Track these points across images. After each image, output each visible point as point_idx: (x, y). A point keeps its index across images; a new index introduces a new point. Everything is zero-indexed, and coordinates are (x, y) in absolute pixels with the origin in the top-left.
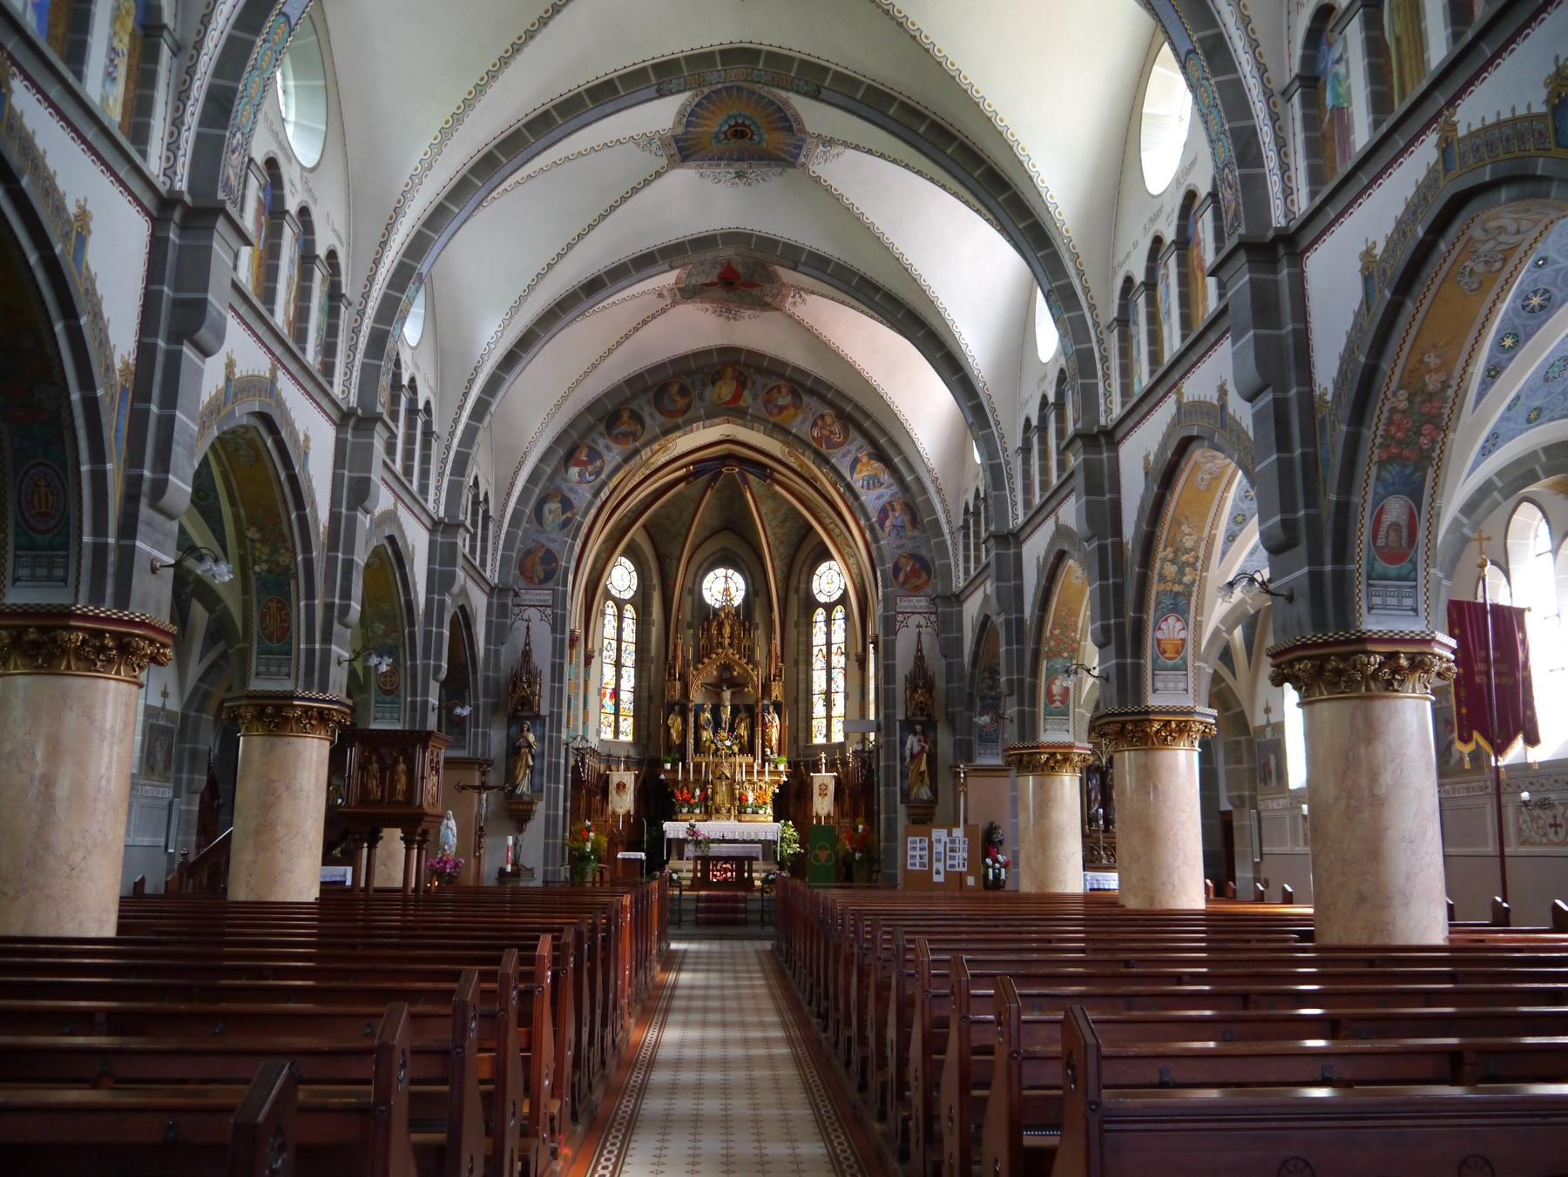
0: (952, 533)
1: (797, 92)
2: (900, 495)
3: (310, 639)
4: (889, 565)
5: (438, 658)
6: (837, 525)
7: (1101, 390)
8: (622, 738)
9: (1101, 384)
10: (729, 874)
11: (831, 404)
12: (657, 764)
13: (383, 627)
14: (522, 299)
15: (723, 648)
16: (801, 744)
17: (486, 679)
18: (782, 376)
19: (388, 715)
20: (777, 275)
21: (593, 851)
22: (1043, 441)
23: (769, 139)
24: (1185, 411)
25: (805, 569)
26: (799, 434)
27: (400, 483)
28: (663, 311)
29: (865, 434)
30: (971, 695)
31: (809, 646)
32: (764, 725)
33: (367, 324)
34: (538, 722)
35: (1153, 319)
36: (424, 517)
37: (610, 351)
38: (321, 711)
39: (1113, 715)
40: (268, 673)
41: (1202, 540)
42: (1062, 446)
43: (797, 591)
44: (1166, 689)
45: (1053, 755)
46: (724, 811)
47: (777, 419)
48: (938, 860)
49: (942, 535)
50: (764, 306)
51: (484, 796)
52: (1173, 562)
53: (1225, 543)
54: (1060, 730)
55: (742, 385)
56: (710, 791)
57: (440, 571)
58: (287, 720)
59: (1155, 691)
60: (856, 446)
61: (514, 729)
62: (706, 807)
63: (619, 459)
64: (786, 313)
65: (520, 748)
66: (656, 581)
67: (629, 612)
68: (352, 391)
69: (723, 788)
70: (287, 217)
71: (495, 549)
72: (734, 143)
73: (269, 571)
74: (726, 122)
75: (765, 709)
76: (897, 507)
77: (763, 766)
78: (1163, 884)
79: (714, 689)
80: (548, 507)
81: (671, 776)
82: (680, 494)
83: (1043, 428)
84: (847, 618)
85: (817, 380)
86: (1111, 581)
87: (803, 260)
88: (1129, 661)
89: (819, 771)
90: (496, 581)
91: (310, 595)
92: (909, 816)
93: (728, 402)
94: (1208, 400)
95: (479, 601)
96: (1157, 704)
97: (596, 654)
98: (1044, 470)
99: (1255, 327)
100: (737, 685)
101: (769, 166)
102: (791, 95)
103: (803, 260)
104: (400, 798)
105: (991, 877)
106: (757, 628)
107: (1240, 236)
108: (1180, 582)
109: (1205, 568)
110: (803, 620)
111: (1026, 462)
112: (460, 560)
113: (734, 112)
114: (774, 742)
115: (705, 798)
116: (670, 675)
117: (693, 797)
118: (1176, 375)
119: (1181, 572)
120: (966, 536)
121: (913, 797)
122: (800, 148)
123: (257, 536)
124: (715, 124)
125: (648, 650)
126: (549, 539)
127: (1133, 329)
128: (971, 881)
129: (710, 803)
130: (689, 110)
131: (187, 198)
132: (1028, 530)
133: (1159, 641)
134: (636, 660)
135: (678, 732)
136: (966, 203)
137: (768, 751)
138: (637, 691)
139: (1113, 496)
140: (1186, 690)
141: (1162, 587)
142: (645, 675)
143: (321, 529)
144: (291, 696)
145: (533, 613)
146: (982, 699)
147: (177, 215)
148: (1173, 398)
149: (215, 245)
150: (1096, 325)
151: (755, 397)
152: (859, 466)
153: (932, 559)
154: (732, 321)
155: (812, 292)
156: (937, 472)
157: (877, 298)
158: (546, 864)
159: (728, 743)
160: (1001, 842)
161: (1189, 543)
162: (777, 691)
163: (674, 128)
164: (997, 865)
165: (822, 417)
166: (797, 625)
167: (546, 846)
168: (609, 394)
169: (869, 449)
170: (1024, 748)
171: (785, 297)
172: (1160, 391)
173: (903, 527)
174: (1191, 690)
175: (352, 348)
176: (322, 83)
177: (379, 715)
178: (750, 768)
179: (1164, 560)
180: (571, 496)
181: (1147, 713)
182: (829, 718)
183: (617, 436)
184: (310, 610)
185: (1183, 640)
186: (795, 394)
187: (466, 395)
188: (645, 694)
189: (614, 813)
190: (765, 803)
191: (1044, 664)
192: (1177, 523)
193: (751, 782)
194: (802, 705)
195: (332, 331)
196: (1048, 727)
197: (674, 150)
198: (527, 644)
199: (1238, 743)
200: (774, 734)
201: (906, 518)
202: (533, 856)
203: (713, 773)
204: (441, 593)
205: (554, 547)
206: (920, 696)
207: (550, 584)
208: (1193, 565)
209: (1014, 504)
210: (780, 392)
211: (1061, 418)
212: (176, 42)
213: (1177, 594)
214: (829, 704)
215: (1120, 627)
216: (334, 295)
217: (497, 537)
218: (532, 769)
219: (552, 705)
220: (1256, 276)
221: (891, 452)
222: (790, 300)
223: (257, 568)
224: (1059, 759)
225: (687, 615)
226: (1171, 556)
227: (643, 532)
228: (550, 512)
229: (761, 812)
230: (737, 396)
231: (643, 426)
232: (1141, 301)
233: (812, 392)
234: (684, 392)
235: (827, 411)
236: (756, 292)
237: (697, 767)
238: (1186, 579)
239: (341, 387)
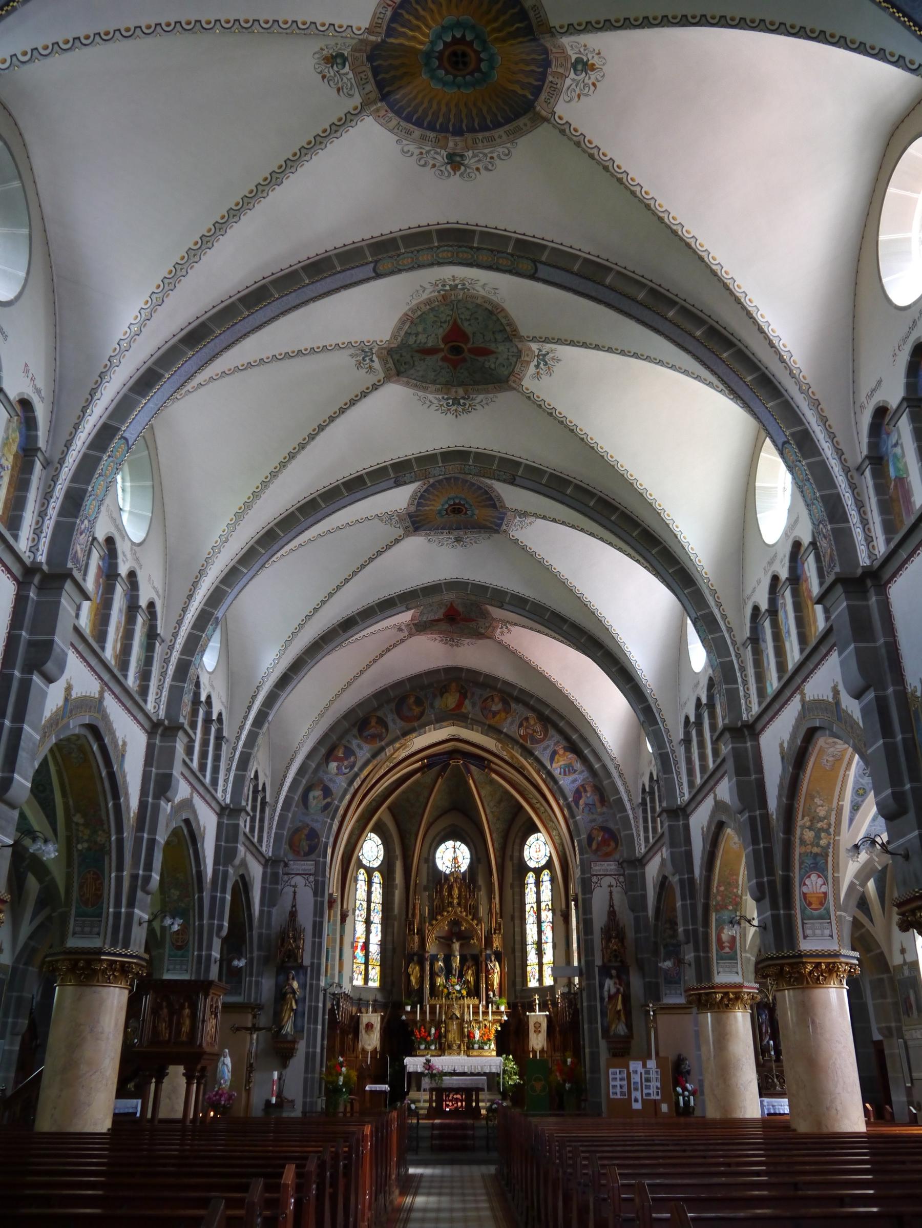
0: (633, 809)
1: (498, 480)
2: (590, 779)
3: (118, 904)
4: (584, 836)
5: (221, 918)
6: (541, 805)
7: (742, 694)
8: (371, 984)
9: (741, 688)
10: (459, 1104)
11: (533, 709)
12: (401, 1007)
13: (177, 893)
14: (294, 634)
15: (453, 906)
16: (518, 987)
17: (260, 935)
18: (494, 688)
19: (178, 967)
20: (488, 613)
21: (345, 1083)
22: (700, 734)
23: (480, 514)
24: (808, 708)
25: (518, 841)
26: (510, 733)
27: (195, 778)
28: (402, 641)
29: (561, 732)
30: (656, 943)
31: (523, 904)
32: (488, 972)
33: (175, 656)
34: (301, 972)
35: (777, 637)
36: (214, 804)
37: (362, 672)
38: (123, 963)
39: (772, 958)
40: (82, 932)
41: (832, 810)
42: (714, 738)
43: (512, 858)
44: (814, 935)
45: (726, 994)
46: (455, 1047)
47: (492, 722)
48: (636, 1089)
49: (626, 811)
50: (480, 636)
51: (255, 1036)
52: (810, 828)
53: (851, 812)
54: (731, 972)
55: (463, 696)
56: (443, 1029)
57: (226, 848)
58: (95, 972)
59: (805, 937)
60: (554, 741)
61: (281, 978)
62: (440, 1044)
63: (368, 755)
64: (496, 641)
65: (285, 994)
66: (398, 852)
67: (377, 878)
68: (162, 707)
69: (454, 1027)
70: (119, 579)
71: (270, 828)
72: (453, 518)
73: (89, 849)
74: (447, 502)
75: (488, 958)
76: (588, 789)
77: (487, 1007)
78: (828, 1109)
79: (446, 941)
80: (311, 795)
81: (411, 1017)
82: (417, 782)
83: (699, 723)
84: (553, 880)
85: (522, 691)
86: (762, 846)
87: (507, 600)
88: (782, 912)
89: (534, 1011)
90: (270, 854)
91: (120, 868)
92: (609, 1049)
93: (453, 709)
94: (825, 698)
95: (256, 871)
96: (808, 948)
97: (350, 913)
98: (702, 757)
99: (855, 641)
100: (464, 938)
101: (480, 532)
102: (494, 482)
103: (507, 600)
104: (184, 1038)
105: (682, 1104)
106: (480, 890)
107: (836, 573)
108: (818, 845)
109: (838, 832)
111: (688, 750)
112: (241, 838)
113: (452, 495)
114: (496, 986)
115: (439, 1036)
117: (429, 1035)
118: (798, 680)
119: (818, 837)
120: (645, 811)
121: (612, 1033)
122: (502, 519)
123: (81, 821)
124: (438, 504)
125: (392, 909)
126: (313, 820)
127: (762, 645)
128: (664, 1108)
129: (443, 1040)
130: (419, 494)
131: (45, 567)
132: (693, 805)
133: (805, 894)
135: (416, 979)
136: (628, 555)
137: (491, 993)
138: (383, 944)
139: (758, 776)
140: (831, 936)
141: (803, 850)
143: (132, 815)
144: (99, 952)
145: (299, 880)
146: (666, 946)
147: (36, 580)
148: (797, 698)
149: (63, 600)
150: (734, 643)
151: (474, 705)
152: (557, 757)
153: (618, 830)
154: (455, 647)
155: (516, 624)
156: (619, 760)
157: (565, 628)
158: (305, 1096)
159: (458, 988)
160: (688, 1072)
161: (822, 813)
162: (497, 943)
163: (408, 507)
164: (686, 1093)
165: (527, 719)
166: (512, 887)
167: (306, 1080)
168: (360, 705)
169: (564, 743)
170: (701, 989)
171: (495, 628)
172: (787, 693)
173: (594, 805)
174: (835, 936)
175: (163, 674)
176: (149, 483)
177: (171, 967)
178: (476, 1008)
179: (803, 827)
180: (331, 785)
181: (800, 956)
182: (541, 964)
183: (366, 738)
184: (119, 880)
185: (825, 894)
186: (505, 702)
187: (249, 708)
188: (390, 946)
189: (363, 1050)
190: (489, 1040)
191: (714, 917)
192: (810, 797)
193: (477, 1022)
194: (518, 954)
195: (148, 661)
196: (721, 970)
197: (409, 524)
198: (294, 906)
199: (881, 980)
200: (496, 979)
201: (597, 798)
202: (295, 1090)
203: (446, 1014)
204: (225, 865)
205: (317, 826)
206: (614, 945)
207: (313, 856)
208: (827, 831)
209: (681, 784)
210: (493, 700)
211: (712, 716)
212: (46, 459)
213: (816, 855)
214: (540, 953)
215: (772, 883)
216: (152, 635)
217: (272, 818)
218: (295, 1012)
219: (313, 957)
220: (851, 603)
221: (581, 745)
222: (499, 630)
223: (80, 847)
224: (732, 996)
225: (424, 879)
226: (808, 824)
227: (388, 812)
228: (314, 798)
229: (486, 1047)
230: (460, 705)
231: (387, 730)
232: (767, 624)
233: (518, 700)
234: (419, 702)
235: (530, 714)
236: (472, 625)
237: (433, 1008)
238: (823, 842)
239: (154, 704)
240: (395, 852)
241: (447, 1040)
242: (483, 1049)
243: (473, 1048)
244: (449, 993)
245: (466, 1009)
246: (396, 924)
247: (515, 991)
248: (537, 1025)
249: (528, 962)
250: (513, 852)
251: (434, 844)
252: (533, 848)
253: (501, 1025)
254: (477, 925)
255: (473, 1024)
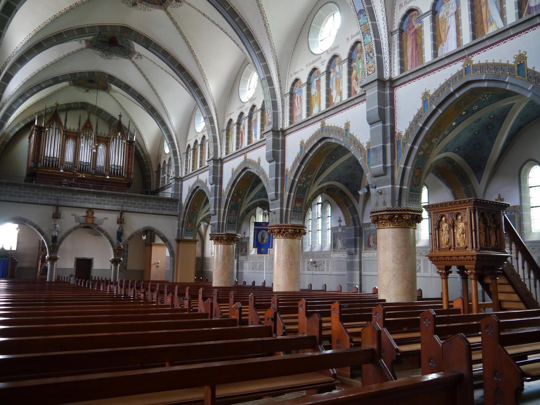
39: (278, 226)
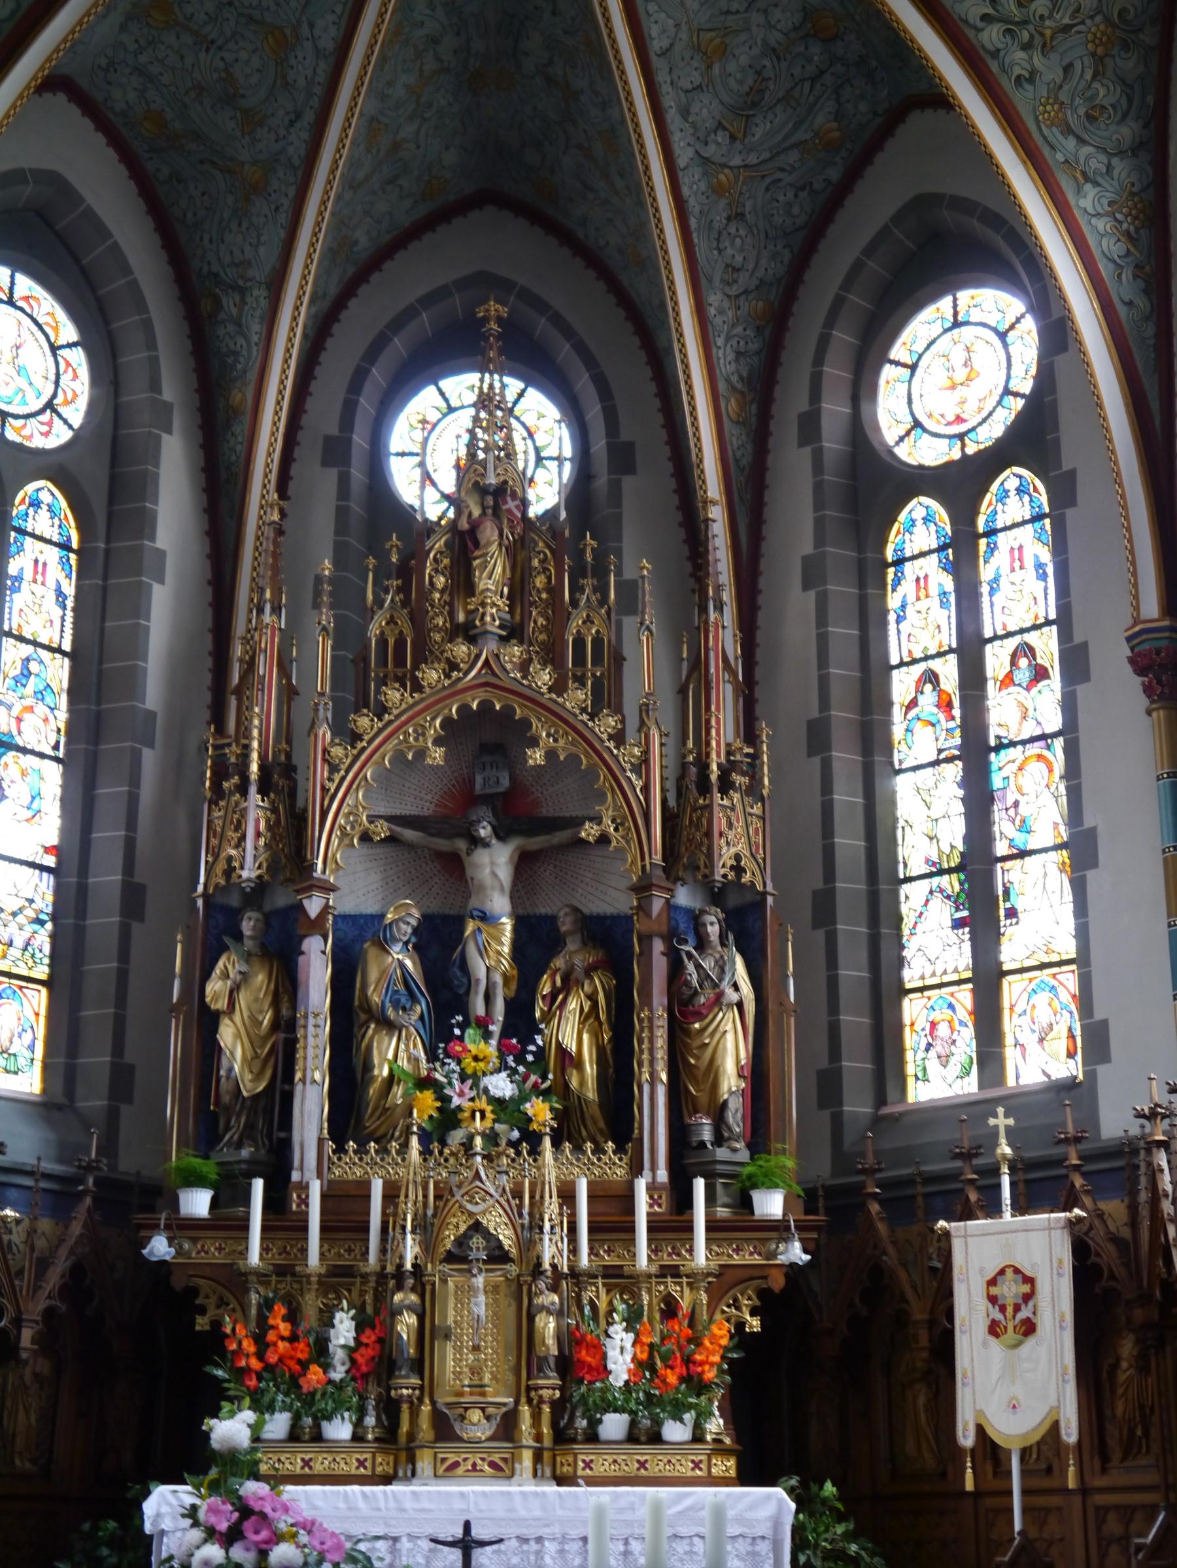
25: (843, 338)
46: (478, 1427)
56: (407, 1323)
62: (390, 1409)
77: (682, 1201)
81: (212, 1252)
110: (839, 553)
114: (730, 1081)
116: (221, 773)
125: (133, 681)
129: (406, 1386)
134: (72, 729)
135: (255, 1042)
142: (110, 791)
159: (501, 1086)
166: (813, 575)
190: (699, 1387)
203: (426, 1229)
229: (676, 1431)
240: (155, 385)
241: (428, 1389)
242: (656, 1438)
243: (592, 1437)
244: (448, 1119)
245: (552, 1207)
246: (150, 759)
247: (837, 1121)
248: (1010, 1290)
249: (911, 977)
250: (815, 395)
251: (378, 376)
252: (931, 375)
253: (766, 1305)
254: (619, 738)
255: (597, 1294)
